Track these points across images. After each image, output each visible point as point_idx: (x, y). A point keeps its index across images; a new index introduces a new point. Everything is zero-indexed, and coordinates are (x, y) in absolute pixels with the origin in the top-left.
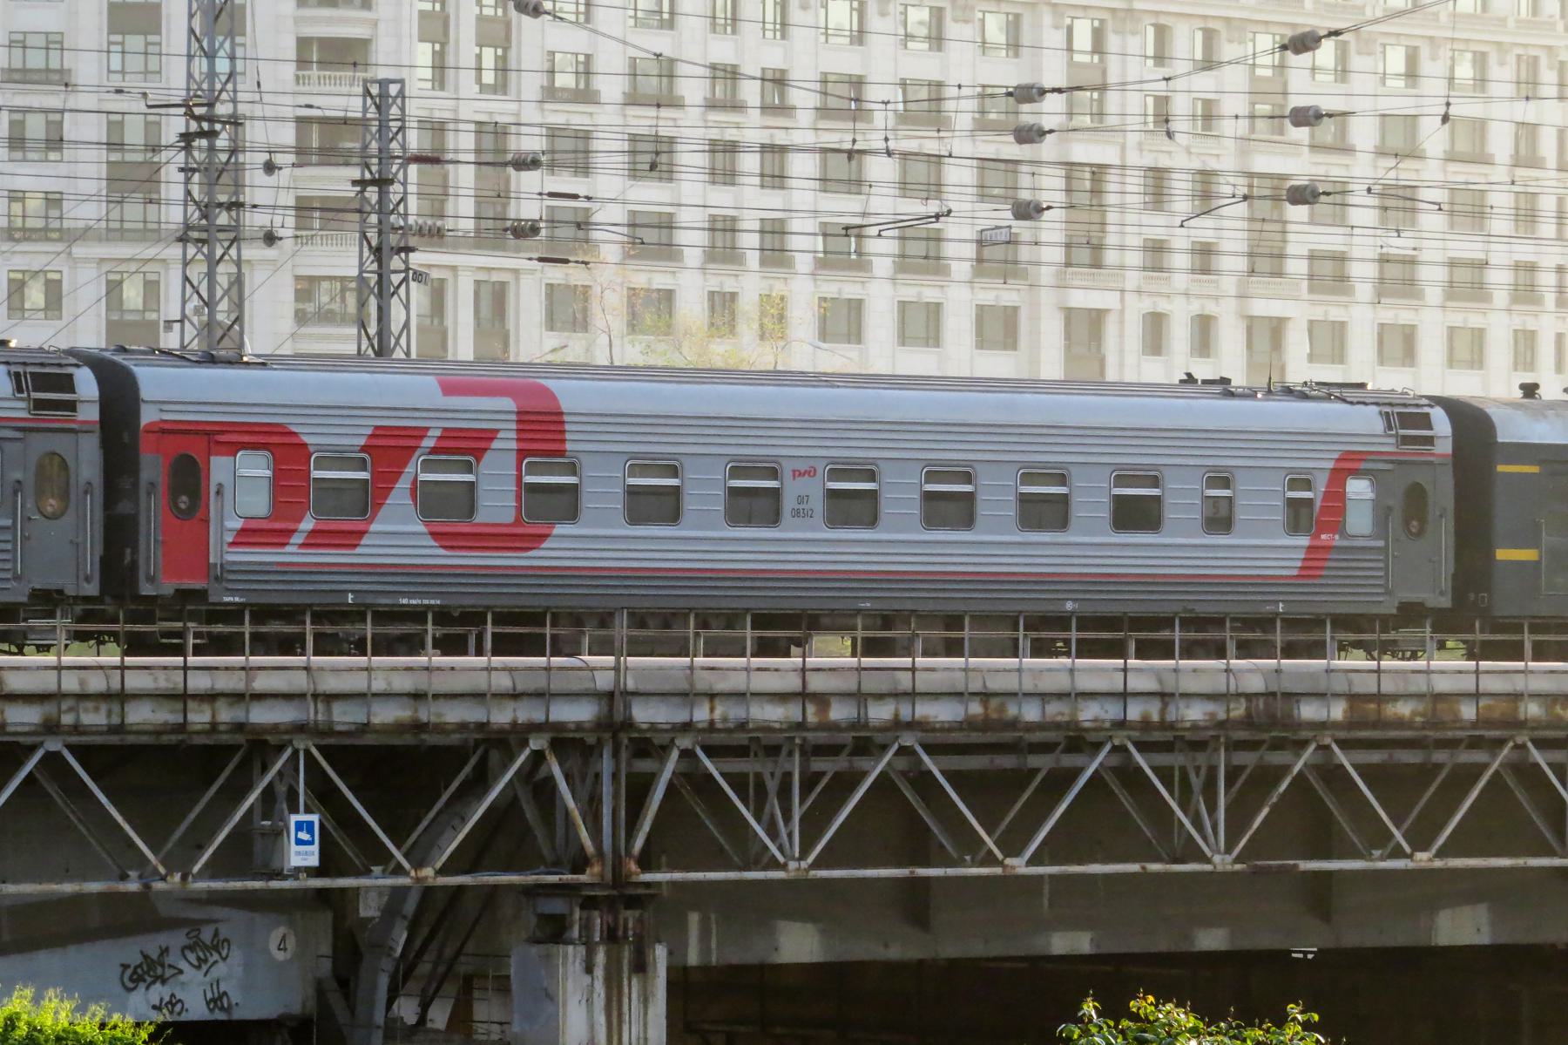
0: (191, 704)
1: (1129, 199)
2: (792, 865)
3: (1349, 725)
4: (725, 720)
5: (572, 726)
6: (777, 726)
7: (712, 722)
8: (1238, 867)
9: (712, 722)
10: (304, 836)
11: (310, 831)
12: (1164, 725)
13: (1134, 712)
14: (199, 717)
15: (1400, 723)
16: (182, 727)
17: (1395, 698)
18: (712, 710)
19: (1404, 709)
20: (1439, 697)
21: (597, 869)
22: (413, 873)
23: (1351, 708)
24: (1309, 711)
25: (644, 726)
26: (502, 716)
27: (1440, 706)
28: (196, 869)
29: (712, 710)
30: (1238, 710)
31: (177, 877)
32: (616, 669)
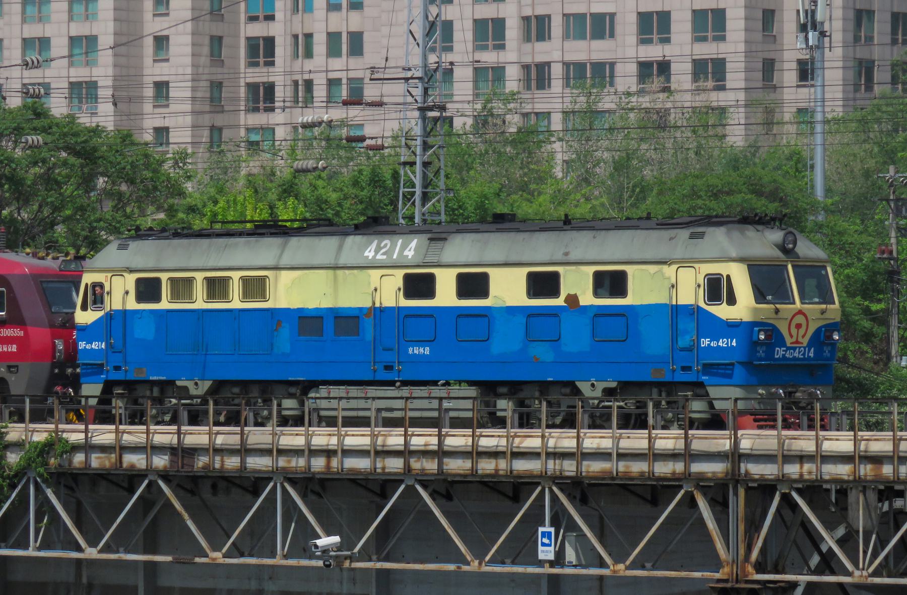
1: (282, 104)
2: (857, 573)
4: (810, 473)
5: (710, 475)
6: (846, 478)
7: (801, 475)
9: (801, 475)
10: (546, 541)
11: (550, 538)
16: (474, 471)
18: (801, 468)
21: (726, 570)
22: (612, 567)
25: (757, 477)
28: (487, 558)
29: (801, 468)
31: (476, 563)
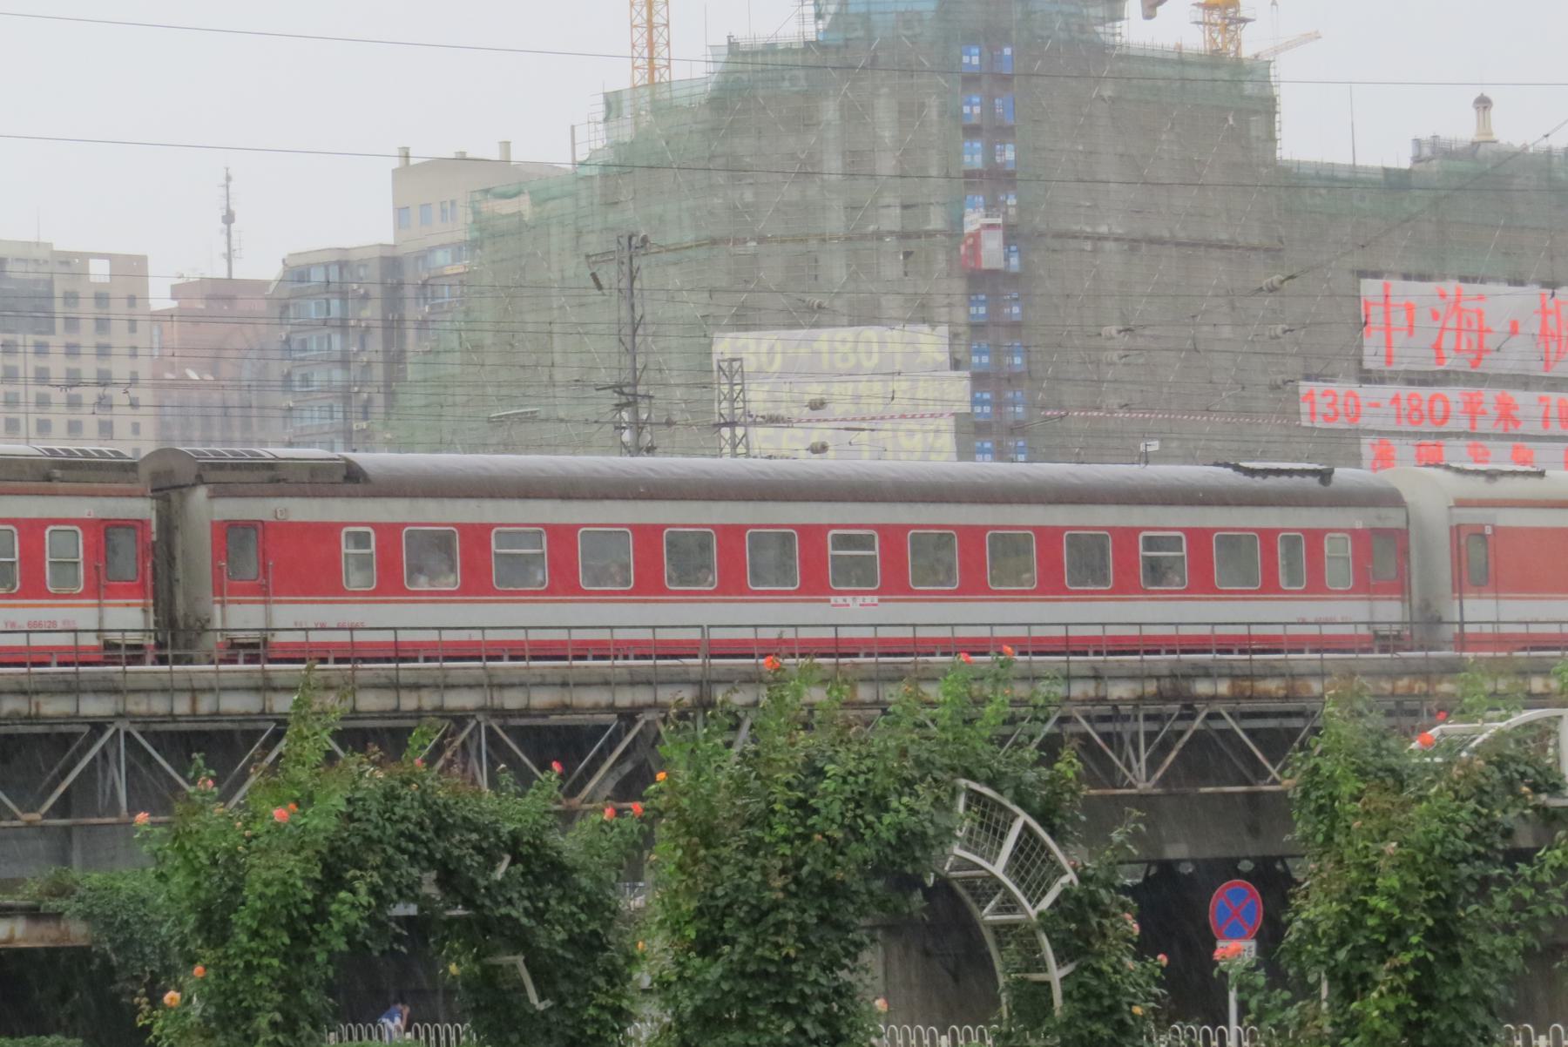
0: (403, 693)
3: (1235, 697)
8: (1158, 791)
12: (1101, 700)
13: (1078, 689)
14: (409, 702)
15: (1269, 696)
17: (1264, 677)
19: (1272, 685)
20: (1292, 676)
23: (1233, 686)
24: (1202, 687)
26: (624, 698)
27: (1298, 683)
30: (1151, 687)
32: (703, 665)
